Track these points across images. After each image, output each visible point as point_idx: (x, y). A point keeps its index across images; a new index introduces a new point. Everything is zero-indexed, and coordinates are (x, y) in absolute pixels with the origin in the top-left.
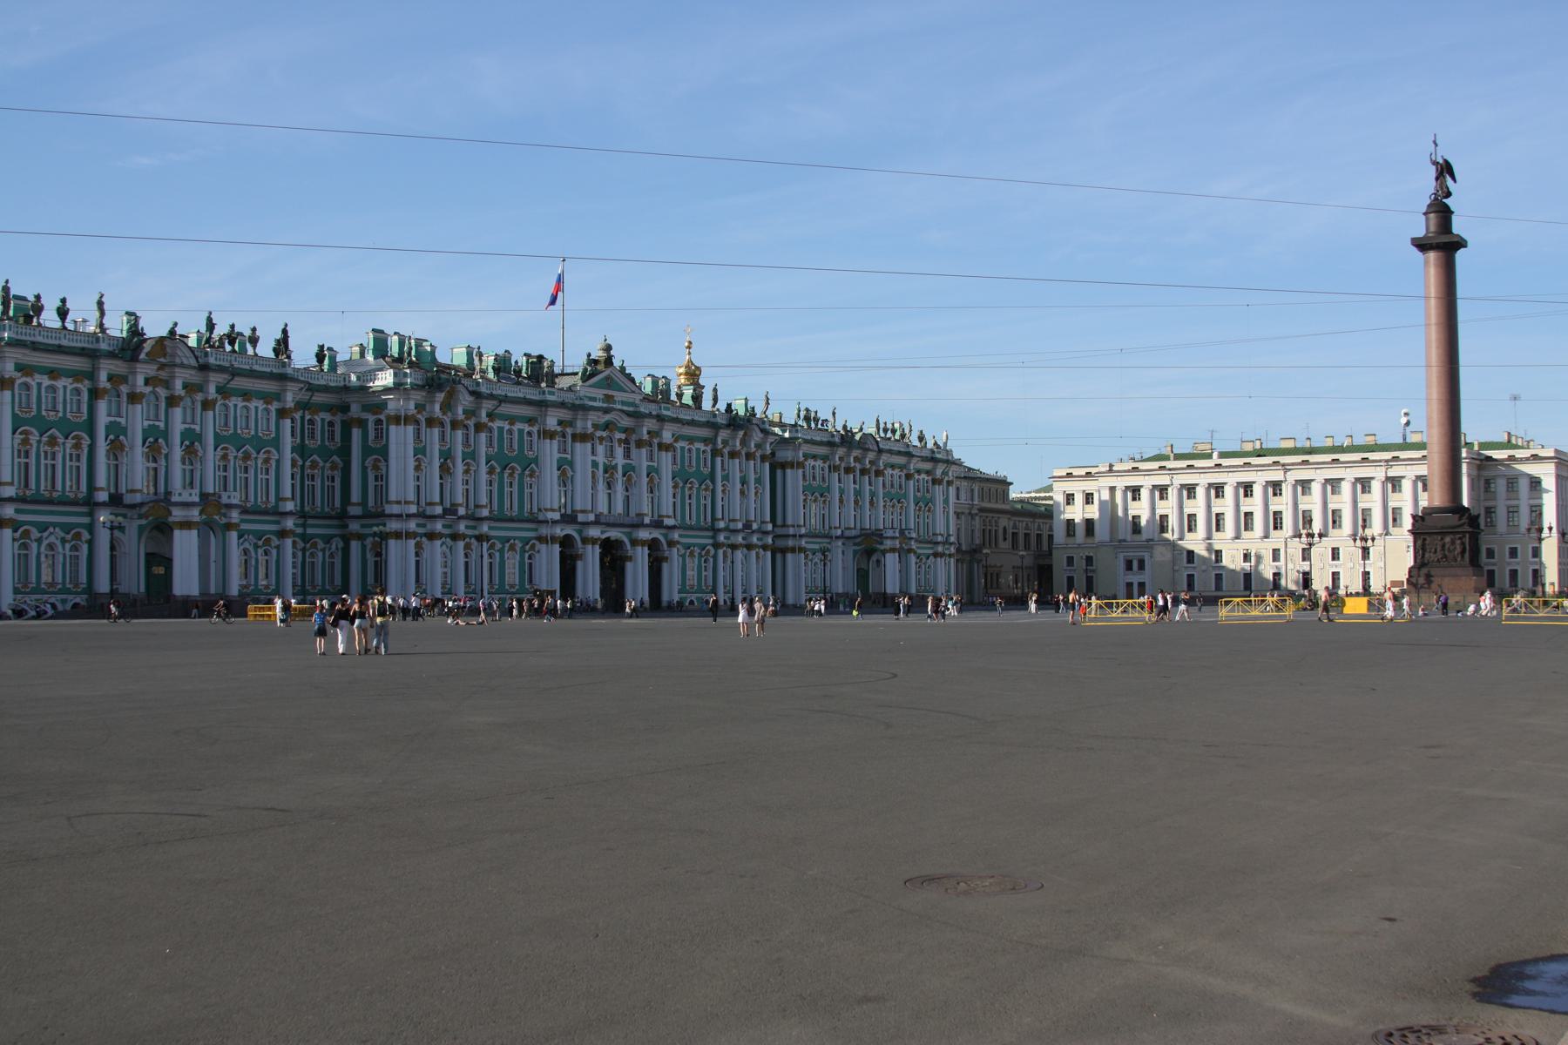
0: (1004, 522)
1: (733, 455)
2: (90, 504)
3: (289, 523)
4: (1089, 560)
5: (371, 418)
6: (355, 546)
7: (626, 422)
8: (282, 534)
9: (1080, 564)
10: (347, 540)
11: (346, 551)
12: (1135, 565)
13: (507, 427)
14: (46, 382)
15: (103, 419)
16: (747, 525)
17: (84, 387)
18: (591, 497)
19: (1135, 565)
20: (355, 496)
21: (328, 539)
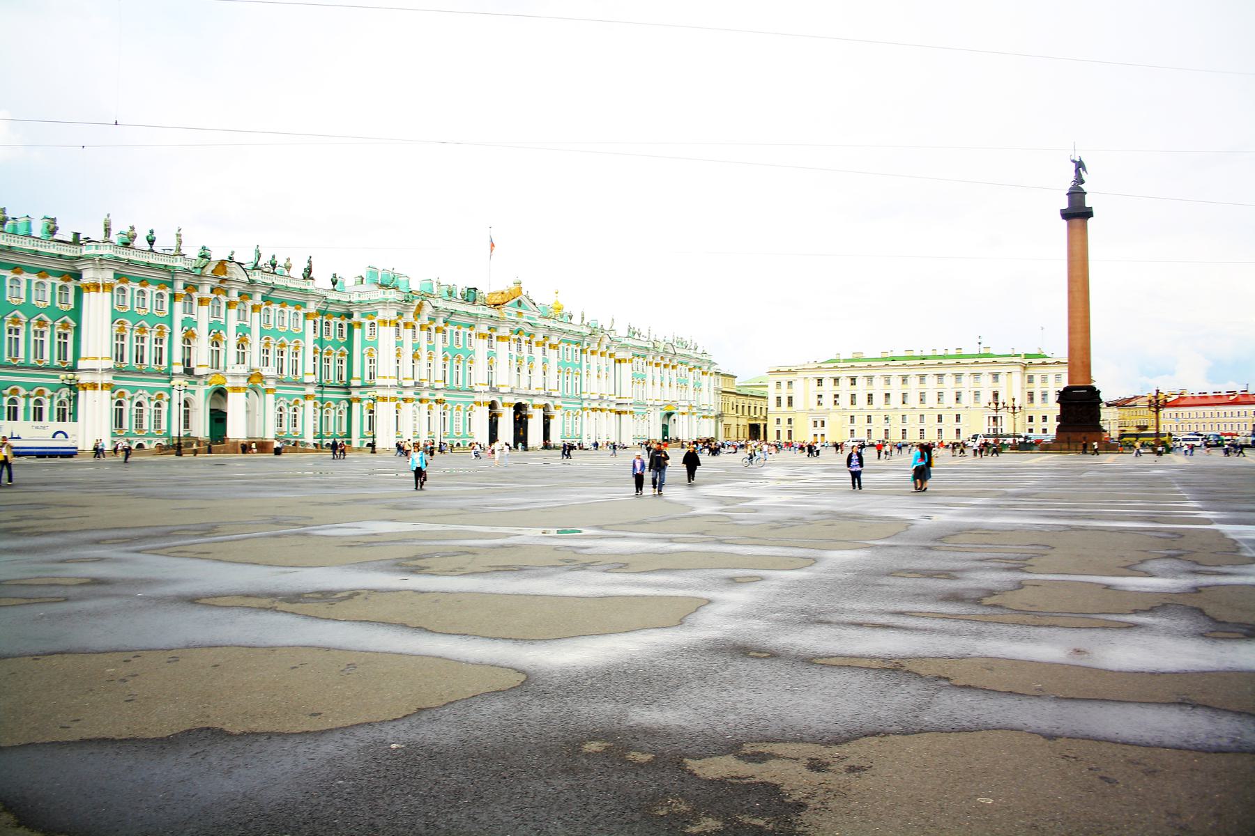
0: (733, 399)
1: (592, 352)
2: (170, 375)
3: (310, 390)
4: (790, 421)
5: (367, 322)
6: (356, 406)
7: (528, 329)
8: (306, 397)
9: (784, 422)
10: (350, 402)
11: (350, 409)
12: (819, 424)
13: (456, 330)
14: (138, 287)
15: (179, 314)
16: (601, 398)
17: (167, 293)
18: (505, 377)
19: (819, 424)
20: (356, 373)
21: (338, 402)
